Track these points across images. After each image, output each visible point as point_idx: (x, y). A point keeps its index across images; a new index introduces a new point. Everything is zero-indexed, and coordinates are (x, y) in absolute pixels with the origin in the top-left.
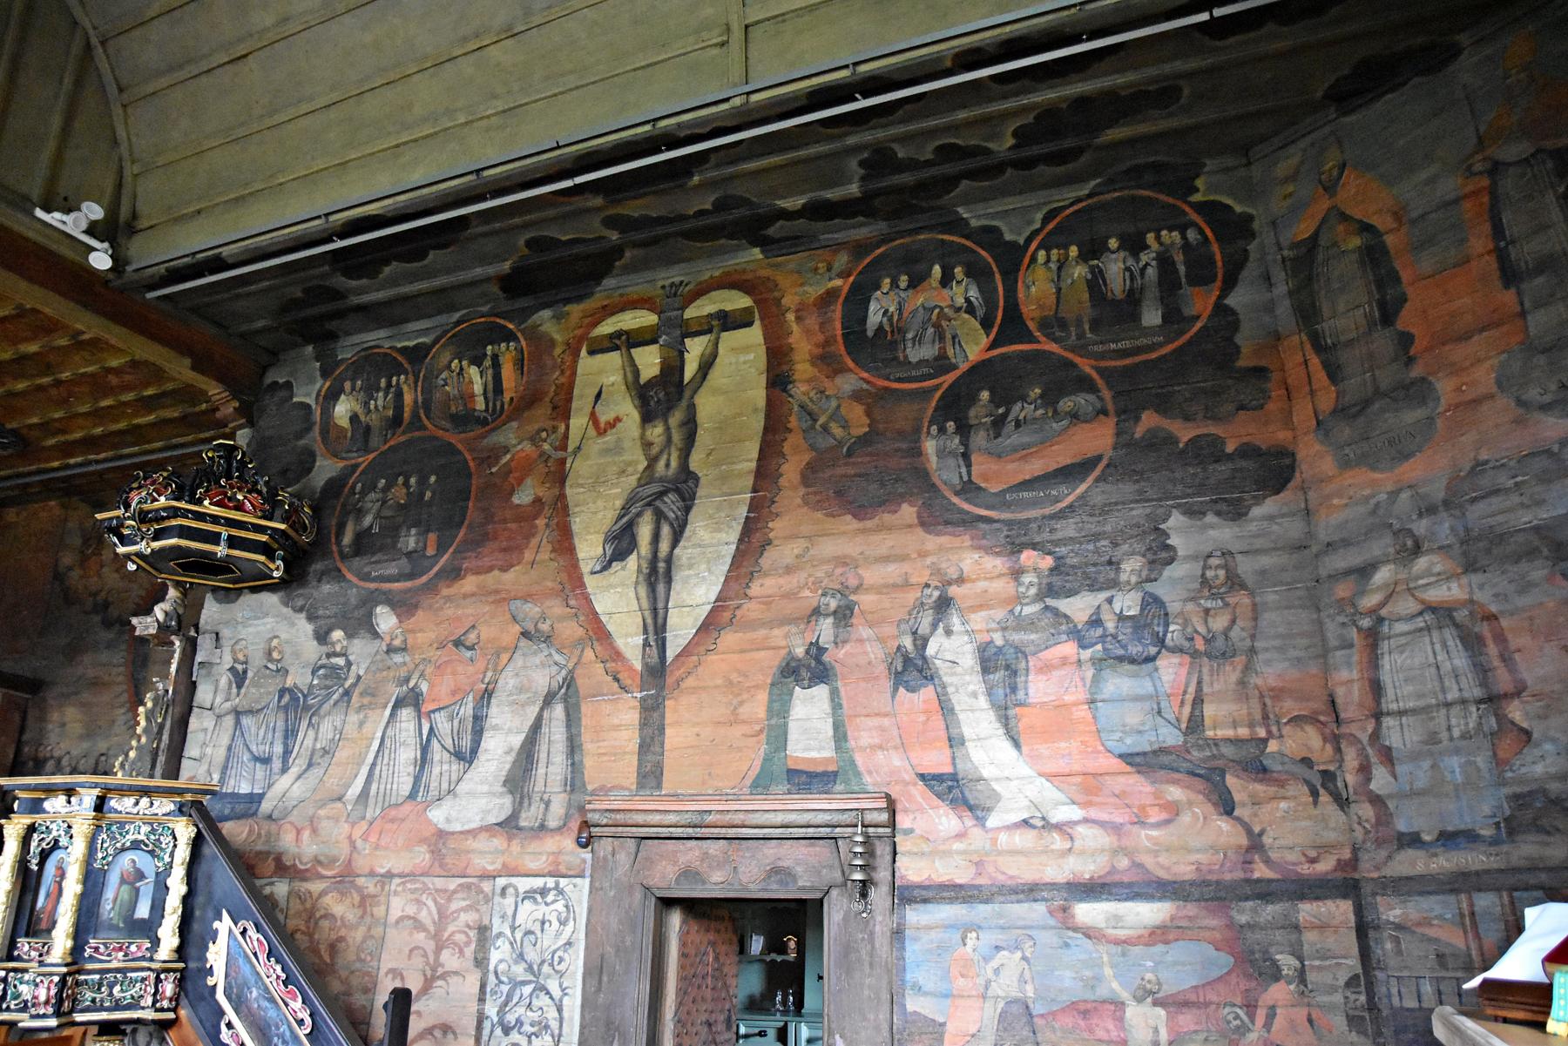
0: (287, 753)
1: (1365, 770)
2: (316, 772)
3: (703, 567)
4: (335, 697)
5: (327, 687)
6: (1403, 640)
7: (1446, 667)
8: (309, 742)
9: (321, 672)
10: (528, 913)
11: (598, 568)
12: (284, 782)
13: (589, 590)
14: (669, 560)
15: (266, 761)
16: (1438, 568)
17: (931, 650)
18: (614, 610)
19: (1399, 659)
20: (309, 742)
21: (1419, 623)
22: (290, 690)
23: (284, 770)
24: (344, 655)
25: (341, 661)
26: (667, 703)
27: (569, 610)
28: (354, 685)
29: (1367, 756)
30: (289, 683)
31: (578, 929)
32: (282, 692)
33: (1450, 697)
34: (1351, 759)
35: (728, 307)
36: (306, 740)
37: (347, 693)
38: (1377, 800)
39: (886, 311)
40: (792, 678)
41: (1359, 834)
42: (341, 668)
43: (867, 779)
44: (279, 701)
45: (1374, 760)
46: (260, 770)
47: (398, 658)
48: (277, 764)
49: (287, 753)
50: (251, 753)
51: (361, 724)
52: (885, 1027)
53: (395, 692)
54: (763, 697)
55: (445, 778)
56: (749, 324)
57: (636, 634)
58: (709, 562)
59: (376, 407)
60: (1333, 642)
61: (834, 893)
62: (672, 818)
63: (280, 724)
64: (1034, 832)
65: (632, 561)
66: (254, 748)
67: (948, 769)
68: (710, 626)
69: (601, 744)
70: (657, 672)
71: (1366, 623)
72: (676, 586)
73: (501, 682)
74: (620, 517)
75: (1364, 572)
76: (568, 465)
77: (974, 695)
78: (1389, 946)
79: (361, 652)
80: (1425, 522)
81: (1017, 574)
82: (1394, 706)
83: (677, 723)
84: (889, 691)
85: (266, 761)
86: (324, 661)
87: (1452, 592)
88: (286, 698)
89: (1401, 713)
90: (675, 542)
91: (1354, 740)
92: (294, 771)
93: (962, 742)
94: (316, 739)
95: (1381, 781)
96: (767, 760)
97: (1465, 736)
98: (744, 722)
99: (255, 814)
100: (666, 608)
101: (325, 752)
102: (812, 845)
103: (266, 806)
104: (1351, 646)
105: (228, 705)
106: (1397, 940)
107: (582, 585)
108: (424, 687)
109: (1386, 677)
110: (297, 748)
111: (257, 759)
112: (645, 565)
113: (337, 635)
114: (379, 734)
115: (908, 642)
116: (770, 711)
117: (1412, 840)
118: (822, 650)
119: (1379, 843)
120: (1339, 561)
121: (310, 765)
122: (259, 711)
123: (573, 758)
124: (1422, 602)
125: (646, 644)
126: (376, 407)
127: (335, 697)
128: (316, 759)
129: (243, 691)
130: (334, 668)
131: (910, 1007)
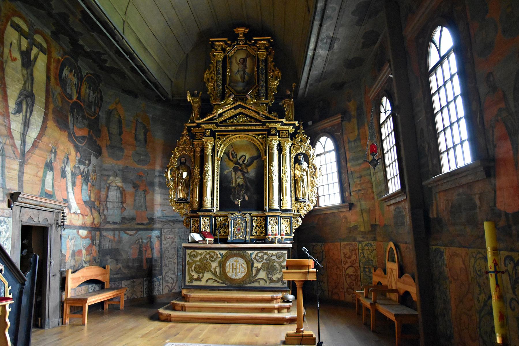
1: (103, 210)
3: (35, 127)
6: (113, 190)
7: (118, 196)
11: (13, 112)
13: (11, 119)
14: (29, 120)
16: (119, 180)
17: (66, 170)
18: (15, 129)
19: (112, 193)
21: (115, 188)
26: (25, 165)
27: (4, 123)
29: (104, 208)
31: (9, 234)
33: (117, 201)
34: (102, 207)
35: (43, 44)
38: (105, 215)
39: (65, 75)
40: (47, 168)
41: (101, 221)
43: (57, 198)
45: (105, 208)
52: (59, 257)
54: (42, 171)
56: (45, 54)
57: (19, 140)
58: (36, 126)
60: (102, 187)
61: (53, 225)
62: (34, 203)
64: (75, 215)
65: (21, 114)
67: (66, 199)
68: (35, 145)
69: (10, 174)
70: (23, 154)
71: (108, 185)
72: (29, 129)
74: (19, 98)
75: (109, 176)
76: (4, 66)
77: (70, 182)
78: (103, 239)
80: (119, 172)
81: (77, 156)
82: (109, 200)
83: (26, 173)
84: (60, 178)
87: (120, 184)
89: (110, 202)
90: (30, 115)
91: (103, 205)
93: (68, 193)
95: (105, 212)
96: (42, 189)
97: (118, 207)
98: (38, 177)
100: (26, 135)
102: (50, 213)
104: (105, 188)
106: (104, 238)
107: (9, 116)
109: (109, 195)
112: (24, 119)
115: (63, 166)
116: (43, 177)
117: (109, 223)
118: (52, 162)
119: (104, 223)
120: (106, 173)
123: (3, 177)
124: (116, 185)
125: (21, 145)
131: (62, 252)
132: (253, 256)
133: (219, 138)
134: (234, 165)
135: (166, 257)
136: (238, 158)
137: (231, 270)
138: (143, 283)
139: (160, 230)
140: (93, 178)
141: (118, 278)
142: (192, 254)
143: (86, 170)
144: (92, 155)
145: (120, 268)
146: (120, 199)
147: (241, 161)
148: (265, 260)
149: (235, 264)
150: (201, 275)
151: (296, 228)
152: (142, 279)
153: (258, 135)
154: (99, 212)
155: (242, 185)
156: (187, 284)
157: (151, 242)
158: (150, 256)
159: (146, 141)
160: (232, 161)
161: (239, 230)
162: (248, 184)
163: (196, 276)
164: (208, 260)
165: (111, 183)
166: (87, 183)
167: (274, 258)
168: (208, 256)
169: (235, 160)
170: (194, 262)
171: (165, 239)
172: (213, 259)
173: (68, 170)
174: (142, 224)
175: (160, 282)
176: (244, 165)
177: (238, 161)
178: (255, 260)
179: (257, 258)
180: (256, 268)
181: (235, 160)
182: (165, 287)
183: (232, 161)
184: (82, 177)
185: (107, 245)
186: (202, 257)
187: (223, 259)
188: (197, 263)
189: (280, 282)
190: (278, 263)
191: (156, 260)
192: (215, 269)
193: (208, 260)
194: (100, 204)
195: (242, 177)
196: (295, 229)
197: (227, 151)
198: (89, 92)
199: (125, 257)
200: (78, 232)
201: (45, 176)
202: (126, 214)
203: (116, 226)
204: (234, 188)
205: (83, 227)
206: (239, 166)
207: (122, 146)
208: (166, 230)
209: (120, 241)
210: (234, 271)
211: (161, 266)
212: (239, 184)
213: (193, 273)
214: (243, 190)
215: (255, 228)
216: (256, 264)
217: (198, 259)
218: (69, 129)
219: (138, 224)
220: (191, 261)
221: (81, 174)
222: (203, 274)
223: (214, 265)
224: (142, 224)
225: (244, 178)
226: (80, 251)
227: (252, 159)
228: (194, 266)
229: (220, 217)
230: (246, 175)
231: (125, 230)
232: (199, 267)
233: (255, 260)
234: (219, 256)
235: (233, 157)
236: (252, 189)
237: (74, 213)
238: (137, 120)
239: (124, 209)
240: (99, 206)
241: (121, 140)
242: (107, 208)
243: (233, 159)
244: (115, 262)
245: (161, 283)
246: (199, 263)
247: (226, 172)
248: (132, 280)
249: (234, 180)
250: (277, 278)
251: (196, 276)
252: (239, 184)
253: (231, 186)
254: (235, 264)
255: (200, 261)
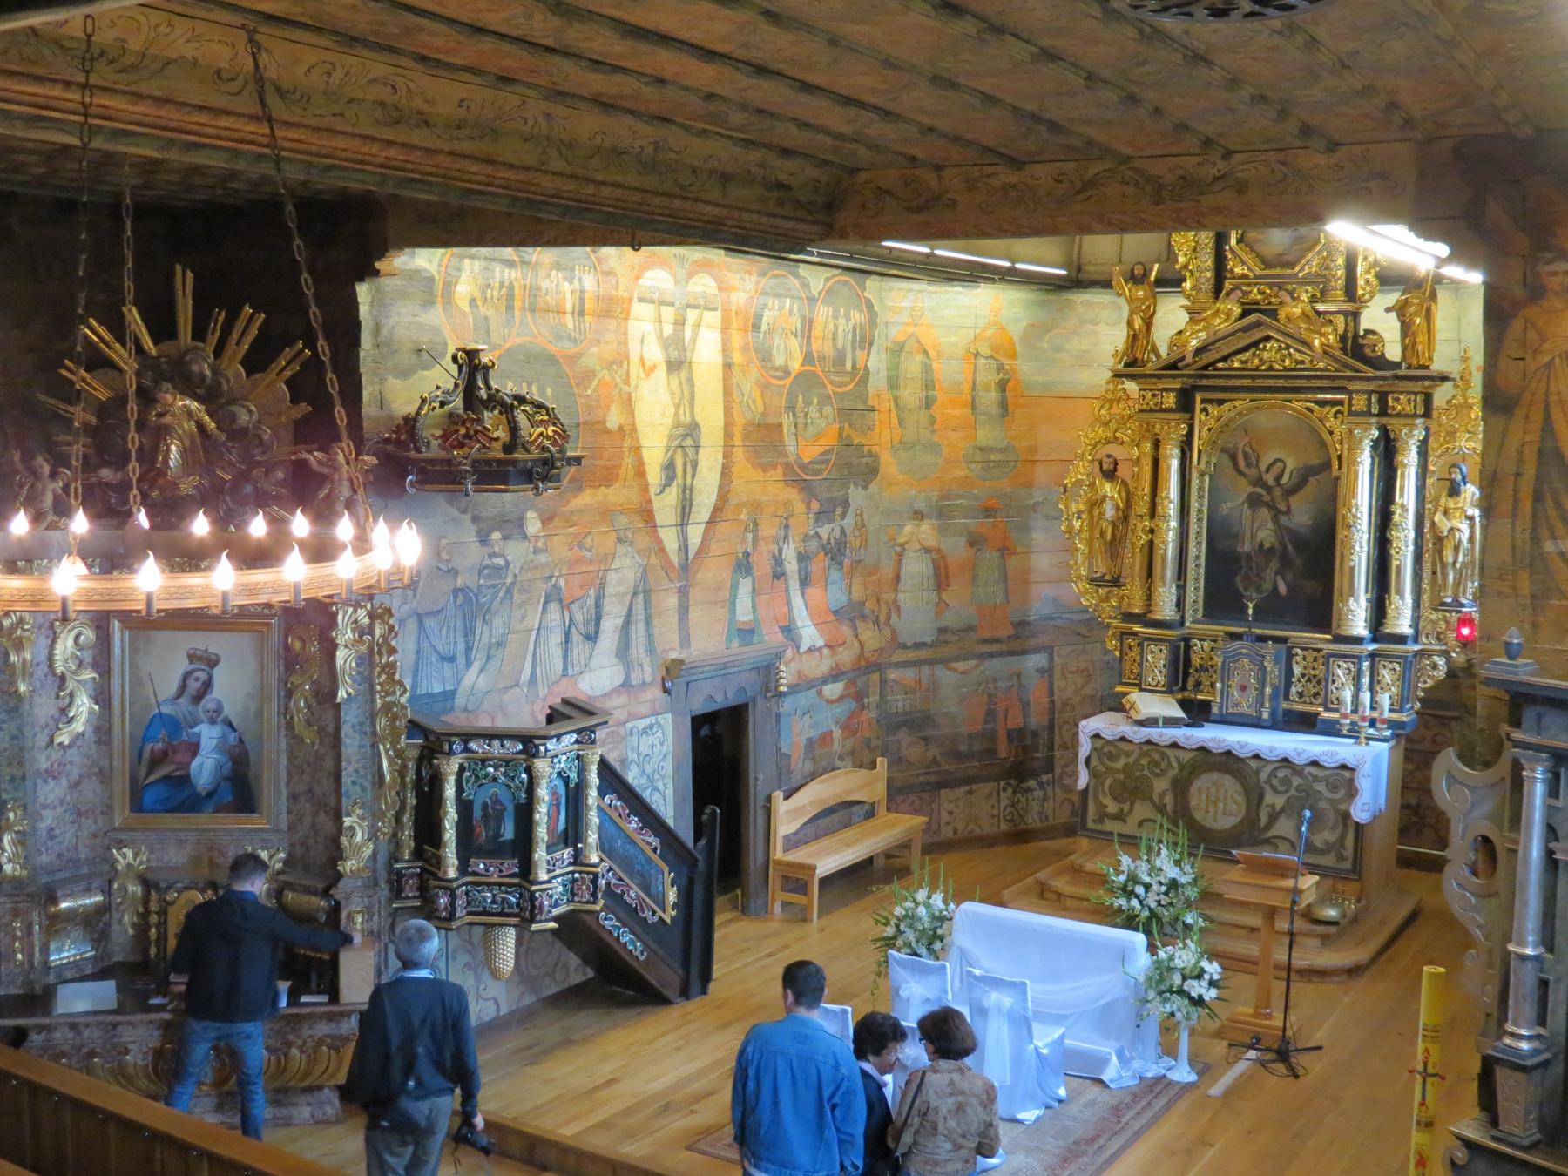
0: (468, 649)
2: (495, 664)
4: (501, 594)
5: (494, 586)
8: (485, 637)
9: (486, 571)
10: (646, 742)
12: (470, 677)
15: (452, 659)
20: (485, 637)
22: (462, 590)
23: (469, 664)
24: (503, 556)
25: (500, 561)
28: (513, 583)
30: (460, 582)
32: (456, 591)
36: (483, 636)
37: (509, 592)
42: (500, 568)
44: (455, 602)
46: (448, 669)
47: (542, 558)
48: (461, 660)
49: (468, 649)
50: (439, 653)
51: (523, 618)
53: (544, 588)
55: (582, 657)
59: (492, 297)
63: (459, 623)
65: (675, 483)
66: (440, 648)
73: (608, 578)
79: (516, 552)
85: (452, 659)
86: (487, 562)
88: (460, 599)
92: (476, 666)
94: (491, 637)
99: (452, 709)
101: (499, 644)
103: (459, 701)
105: (406, 608)
108: (562, 583)
110: (476, 644)
111: (443, 658)
113: (496, 536)
114: (537, 626)
121: (489, 658)
122: (438, 612)
126: (492, 297)
127: (501, 594)
128: (492, 652)
129: (419, 592)
130: (496, 568)
132: (1264, 775)
133: (1204, 410)
134: (1250, 489)
135: (1066, 723)
136: (1263, 469)
137: (1203, 805)
138: (999, 795)
139: (1049, 650)
140: (858, 544)
141: (928, 784)
142: (1105, 750)
143: (837, 533)
144: (852, 487)
145: (934, 759)
146: (932, 580)
147: (1270, 479)
148: (1296, 789)
149: (1213, 790)
150: (1126, 807)
151: (1427, 686)
152: (994, 784)
153: (1322, 403)
154: (876, 622)
155: (1272, 549)
156: (1090, 825)
157: (1021, 685)
158: (1016, 721)
159: (1004, 405)
160: (1244, 475)
161: (1243, 688)
162: (1290, 547)
163: (1112, 808)
164: (1146, 772)
165: (906, 542)
166: (841, 564)
167: (1320, 787)
168: (1144, 761)
169: (1252, 472)
170: (1111, 771)
171: (1063, 674)
172: (1158, 771)
173: (790, 553)
174: (997, 641)
175: (1045, 790)
176: (1277, 489)
177: (1261, 479)
178: (1267, 787)
179: (1275, 782)
180: (1269, 809)
181: (1252, 472)
182: (1062, 804)
183: (1244, 475)
184: (826, 554)
185: (899, 702)
186: (1131, 760)
187: (1185, 773)
188: (1116, 775)
189: (1333, 854)
190: (1330, 801)
191: (1035, 734)
192: (1162, 795)
193: (1146, 772)
194: (878, 601)
195: (1270, 525)
196: (1423, 690)
197: (1231, 445)
198: (835, 325)
199: (947, 730)
200: (820, 693)
201: (735, 587)
202: (949, 619)
203: (923, 654)
204: (1249, 557)
205: (835, 675)
206: (1264, 493)
207: (935, 438)
208: (1066, 650)
209: (934, 688)
210: (1211, 809)
211: (1051, 748)
212: (1261, 545)
213: (1107, 801)
214: (1274, 565)
215: (1299, 681)
216: (1270, 798)
217: (1119, 765)
218: (785, 454)
219: (985, 641)
220: (1102, 769)
221: (824, 549)
222: (1132, 805)
223: (1161, 785)
224: (997, 641)
225: (1279, 528)
226: (826, 738)
227: (1306, 474)
228: (1108, 782)
229: (1201, 640)
230: (1284, 520)
231: (945, 662)
232: (1123, 785)
233: (1267, 787)
234: (1175, 764)
235: (1248, 465)
236: (1299, 562)
237: (810, 650)
238: (977, 355)
239: (942, 605)
240: (876, 609)
241: (933, 421)
242: (898, 608)
243: (1246, 471)
244: (923, 743)
245: (1050, 793)
246: (1121, 777)
247: (1225, 508)
248: (968, 788)
249: (1248, 535)
250: (1327, 843)
251: (1112, 808)
252: (1261, 545)
253: (1239, 549)
254: (1213, 790)
255: (1126, 770)
